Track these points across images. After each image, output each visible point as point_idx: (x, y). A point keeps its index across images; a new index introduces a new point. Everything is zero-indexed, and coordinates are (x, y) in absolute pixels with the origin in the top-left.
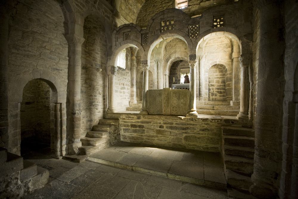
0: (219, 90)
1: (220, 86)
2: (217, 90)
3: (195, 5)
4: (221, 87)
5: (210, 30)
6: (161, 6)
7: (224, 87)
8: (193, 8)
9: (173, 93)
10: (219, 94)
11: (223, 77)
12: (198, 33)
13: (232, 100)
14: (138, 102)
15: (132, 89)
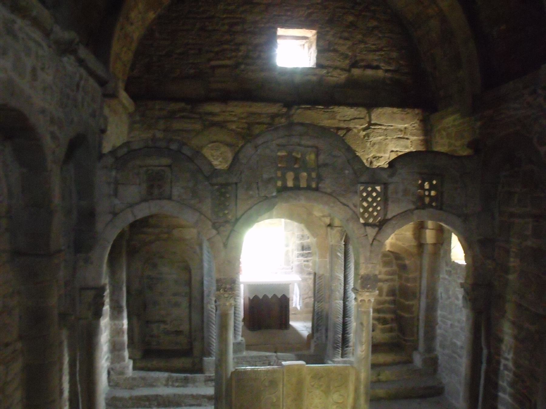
0: (382, 315)
1: (385, 302)
2: (377, 315)
3: (339, 71)
4: (387, 305)
5: (411, 211)
6: (227, 37)
7: (392, 306)
8: (332, 76)
9: (312, 377)
10: (380, 326)
11: (392, 280)
12: (379, 208)
13: (416, 348)
14: (138, 365)
15: (116, 322)
